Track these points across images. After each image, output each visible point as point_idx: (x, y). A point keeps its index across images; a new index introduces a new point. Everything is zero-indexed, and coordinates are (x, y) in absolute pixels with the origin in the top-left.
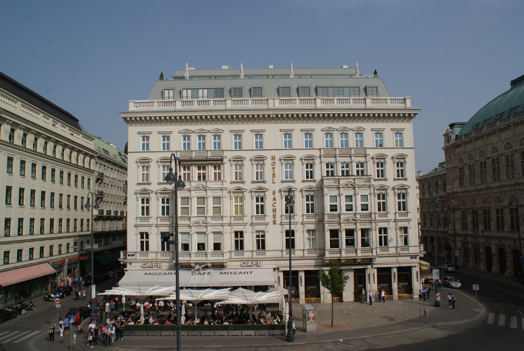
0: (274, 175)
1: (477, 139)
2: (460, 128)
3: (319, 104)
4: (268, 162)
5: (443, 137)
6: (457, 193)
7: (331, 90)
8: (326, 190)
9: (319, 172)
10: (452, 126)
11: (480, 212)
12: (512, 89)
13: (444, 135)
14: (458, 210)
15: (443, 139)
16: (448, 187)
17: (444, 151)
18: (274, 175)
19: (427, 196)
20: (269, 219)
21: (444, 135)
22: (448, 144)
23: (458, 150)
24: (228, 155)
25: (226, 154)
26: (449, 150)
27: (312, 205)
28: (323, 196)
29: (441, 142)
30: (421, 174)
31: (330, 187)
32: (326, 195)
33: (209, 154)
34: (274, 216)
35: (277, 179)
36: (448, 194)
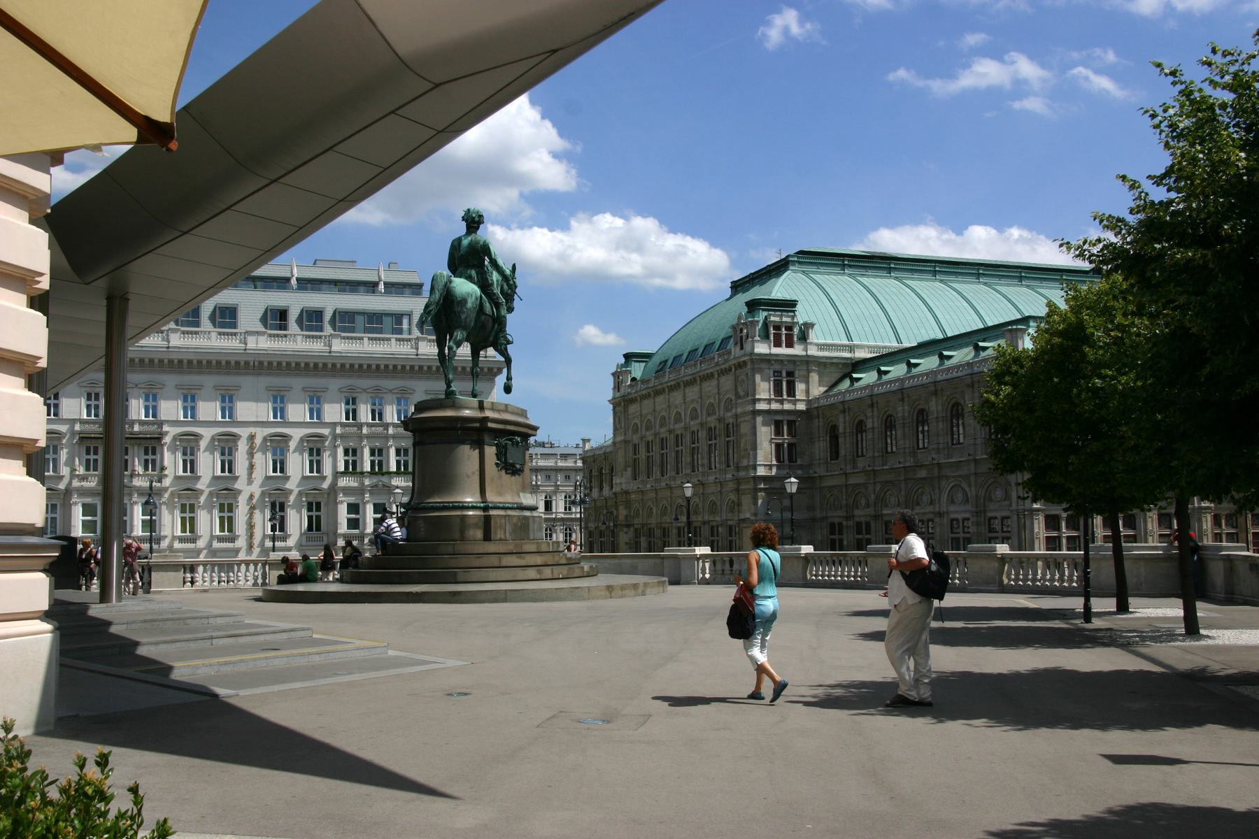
0: (251, 467)
1: (658, 393)
2: (643, 365)
3: (339, 346)
4: (242, 447)
5: (612, 378)
6: (627, 493)
7: (360, 320)
8: (341, 497)
9: (335, 461)
10: (629, 357)
11: (658, 533)
12: (731, 297)
13: (613, 374)
14: (628, 526)
15: (610, 382)
16: (616, 480)
17: (611, 407)
18: (251, 467)
19: (595, 493)
20: (241, 543)
21: (613, 374)
22: (618, 395)
23: (633, 408)
24: (171, 432)
25: (166, 428)
26: (622, 404)
27: (318, 518)
28: (336, 504)
29: (605, 390)
30: (587, 447)
31: (347, 491)
32: (342, 502)
33: (136, 428)
34: (251, 536)
35: (259, 476)
36: (615, 494)
